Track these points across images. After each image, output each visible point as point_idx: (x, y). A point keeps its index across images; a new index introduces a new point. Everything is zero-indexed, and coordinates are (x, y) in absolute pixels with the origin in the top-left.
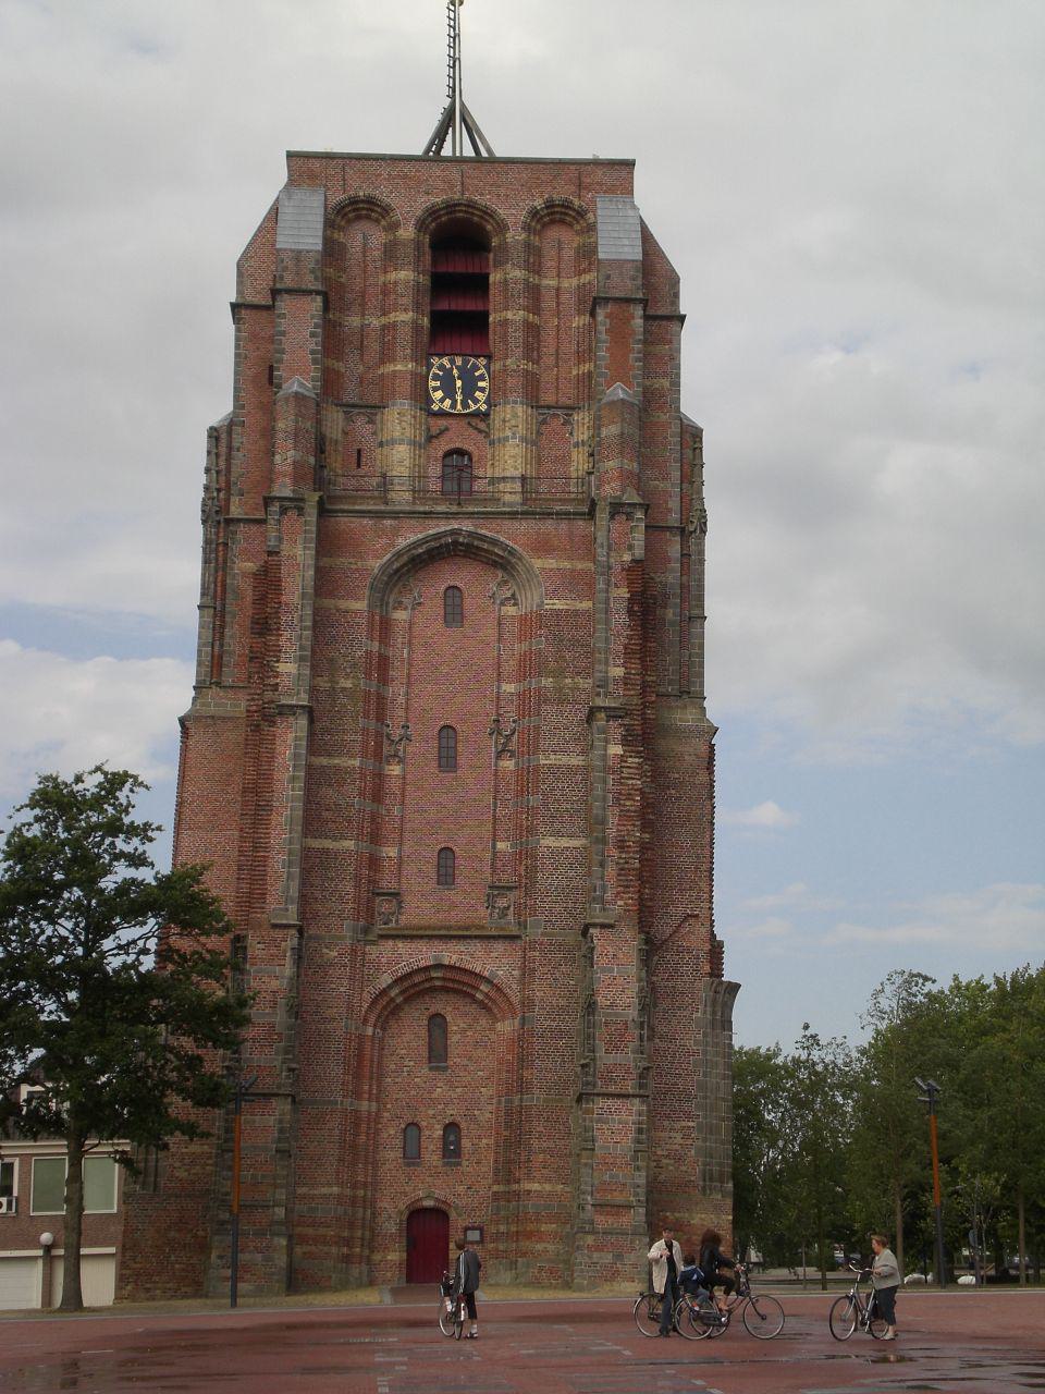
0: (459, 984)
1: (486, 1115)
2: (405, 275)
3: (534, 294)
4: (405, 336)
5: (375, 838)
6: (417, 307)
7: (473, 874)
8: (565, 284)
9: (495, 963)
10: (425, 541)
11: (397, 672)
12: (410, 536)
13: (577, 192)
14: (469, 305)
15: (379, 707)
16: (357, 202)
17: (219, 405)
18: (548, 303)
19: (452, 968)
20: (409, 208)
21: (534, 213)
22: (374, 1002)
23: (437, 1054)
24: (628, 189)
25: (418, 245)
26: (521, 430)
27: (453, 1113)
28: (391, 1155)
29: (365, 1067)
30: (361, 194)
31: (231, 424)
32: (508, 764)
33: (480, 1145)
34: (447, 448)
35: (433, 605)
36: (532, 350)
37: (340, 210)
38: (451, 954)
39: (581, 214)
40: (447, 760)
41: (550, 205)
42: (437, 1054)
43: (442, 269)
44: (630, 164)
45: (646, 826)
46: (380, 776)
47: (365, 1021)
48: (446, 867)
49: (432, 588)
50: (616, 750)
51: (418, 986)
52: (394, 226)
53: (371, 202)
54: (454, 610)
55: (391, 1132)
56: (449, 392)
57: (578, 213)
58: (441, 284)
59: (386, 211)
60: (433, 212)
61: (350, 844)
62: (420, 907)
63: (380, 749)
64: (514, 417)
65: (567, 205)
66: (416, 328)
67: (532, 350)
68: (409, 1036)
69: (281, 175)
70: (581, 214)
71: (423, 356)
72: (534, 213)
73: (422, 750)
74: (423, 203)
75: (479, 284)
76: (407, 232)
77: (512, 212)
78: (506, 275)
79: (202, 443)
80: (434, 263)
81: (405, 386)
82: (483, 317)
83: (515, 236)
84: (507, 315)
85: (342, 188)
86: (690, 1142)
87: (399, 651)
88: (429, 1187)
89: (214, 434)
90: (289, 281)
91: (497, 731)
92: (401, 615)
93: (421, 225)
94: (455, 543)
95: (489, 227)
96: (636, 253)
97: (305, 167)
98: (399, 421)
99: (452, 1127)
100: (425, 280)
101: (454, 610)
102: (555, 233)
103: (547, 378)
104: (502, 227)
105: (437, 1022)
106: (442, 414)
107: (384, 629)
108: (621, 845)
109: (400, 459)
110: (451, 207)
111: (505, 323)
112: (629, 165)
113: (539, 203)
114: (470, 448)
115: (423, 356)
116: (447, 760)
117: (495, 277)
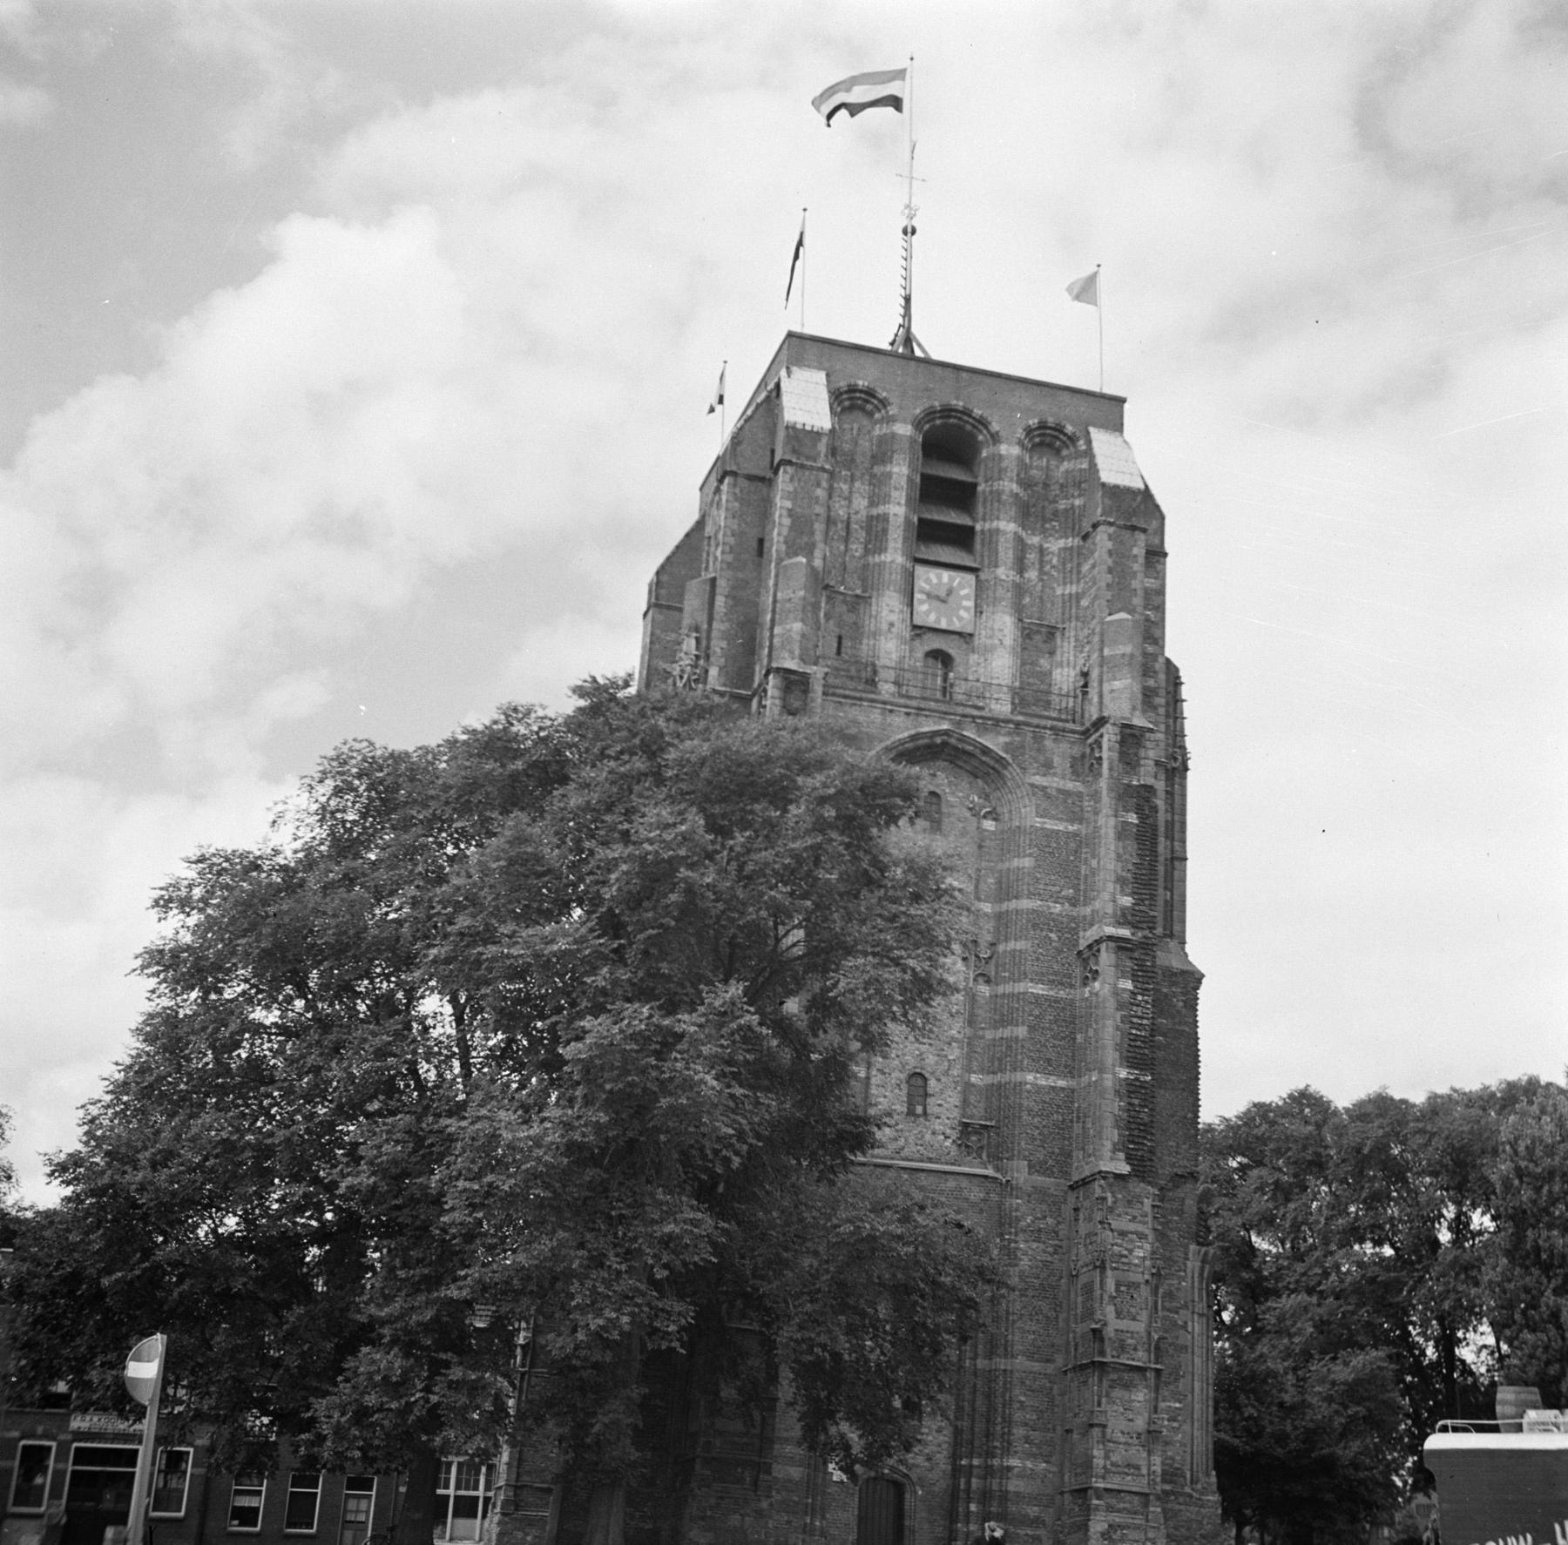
7: (946, 1105)
10: (913, 738)
13: (1066, 422)
16: (855, 391)
21: (1029, 431)
24: (1117, 426)
26: (1008, 641)
30: (860, 383)
34: (927, 648)
44: (1123, 401)
50: (1129, 985)
53: (870, 393)
57: (1070, 438)
76: (904, 429)
81: (897, 577)
86: (1175, 1424)
94: (945, 744)
95: (981, 438)
96: (1142, 486)
104: (995, 438)
110: (947, 411)
112: (1123, 401)
113: (1033, 422)
114: (951, 651)
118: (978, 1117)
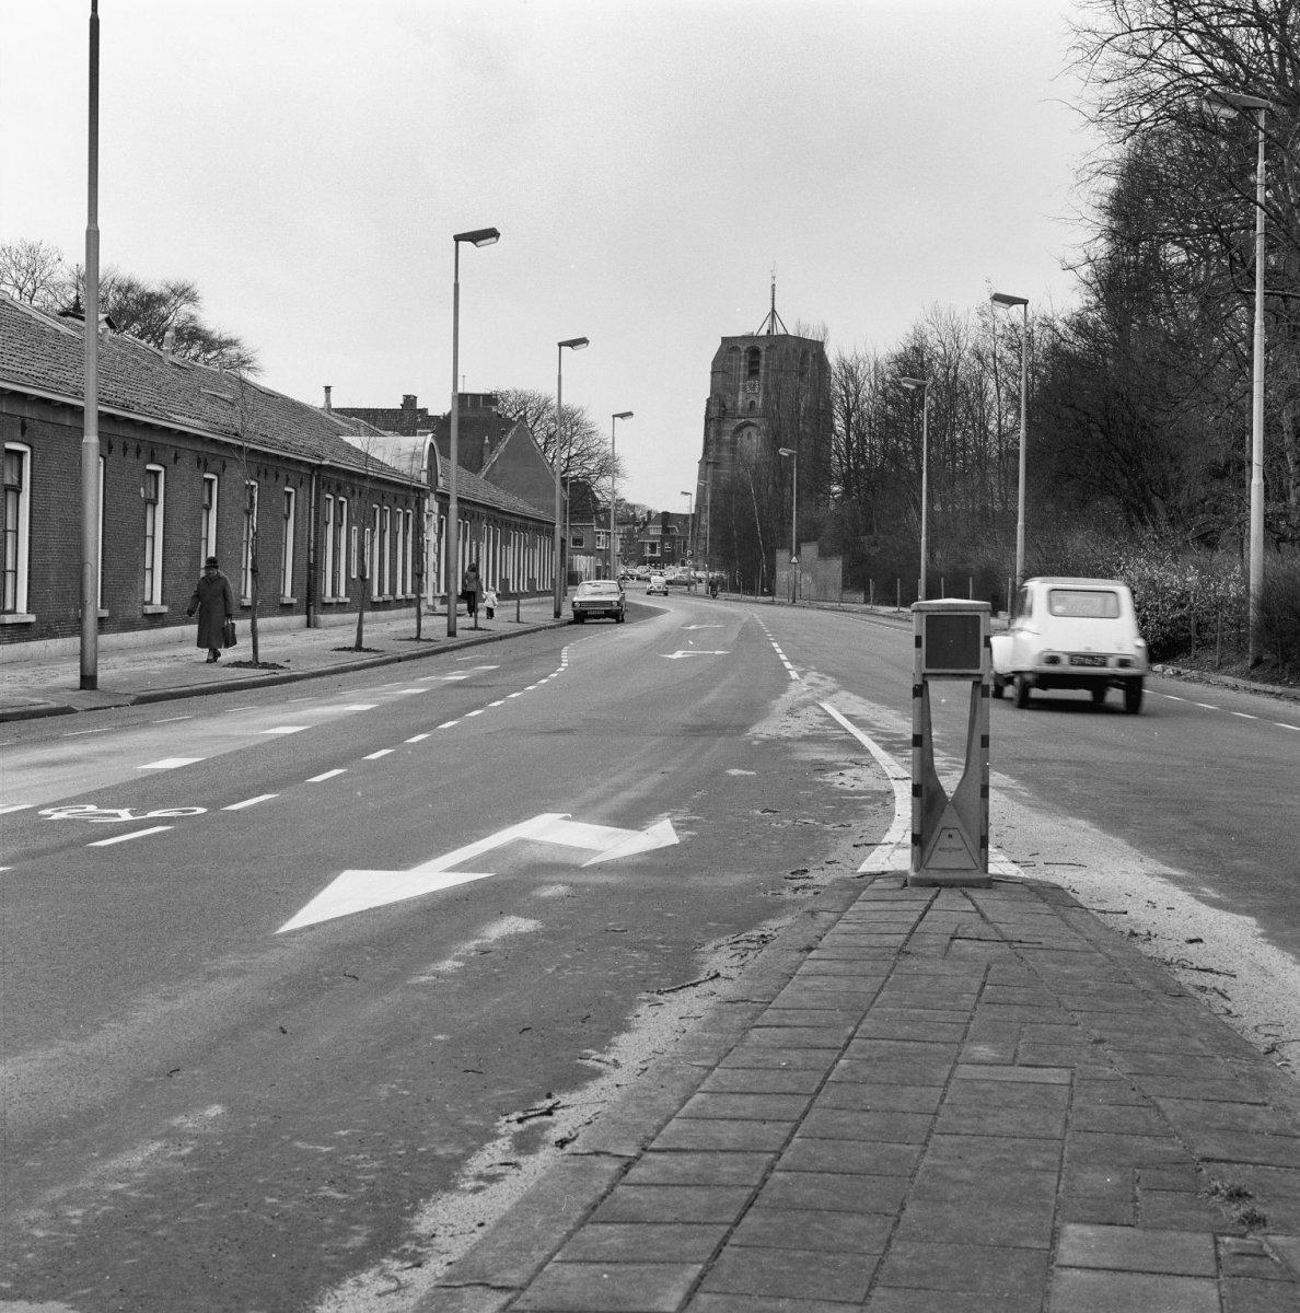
4: (742, 377)
20: (743, 348)
25: (745, 356)
49: (746, 431)
77: (762, 348)
78: (763, 362)
83: (763, 353)
84: (762, 371)
93: (746, 352)
97: (724, 340)
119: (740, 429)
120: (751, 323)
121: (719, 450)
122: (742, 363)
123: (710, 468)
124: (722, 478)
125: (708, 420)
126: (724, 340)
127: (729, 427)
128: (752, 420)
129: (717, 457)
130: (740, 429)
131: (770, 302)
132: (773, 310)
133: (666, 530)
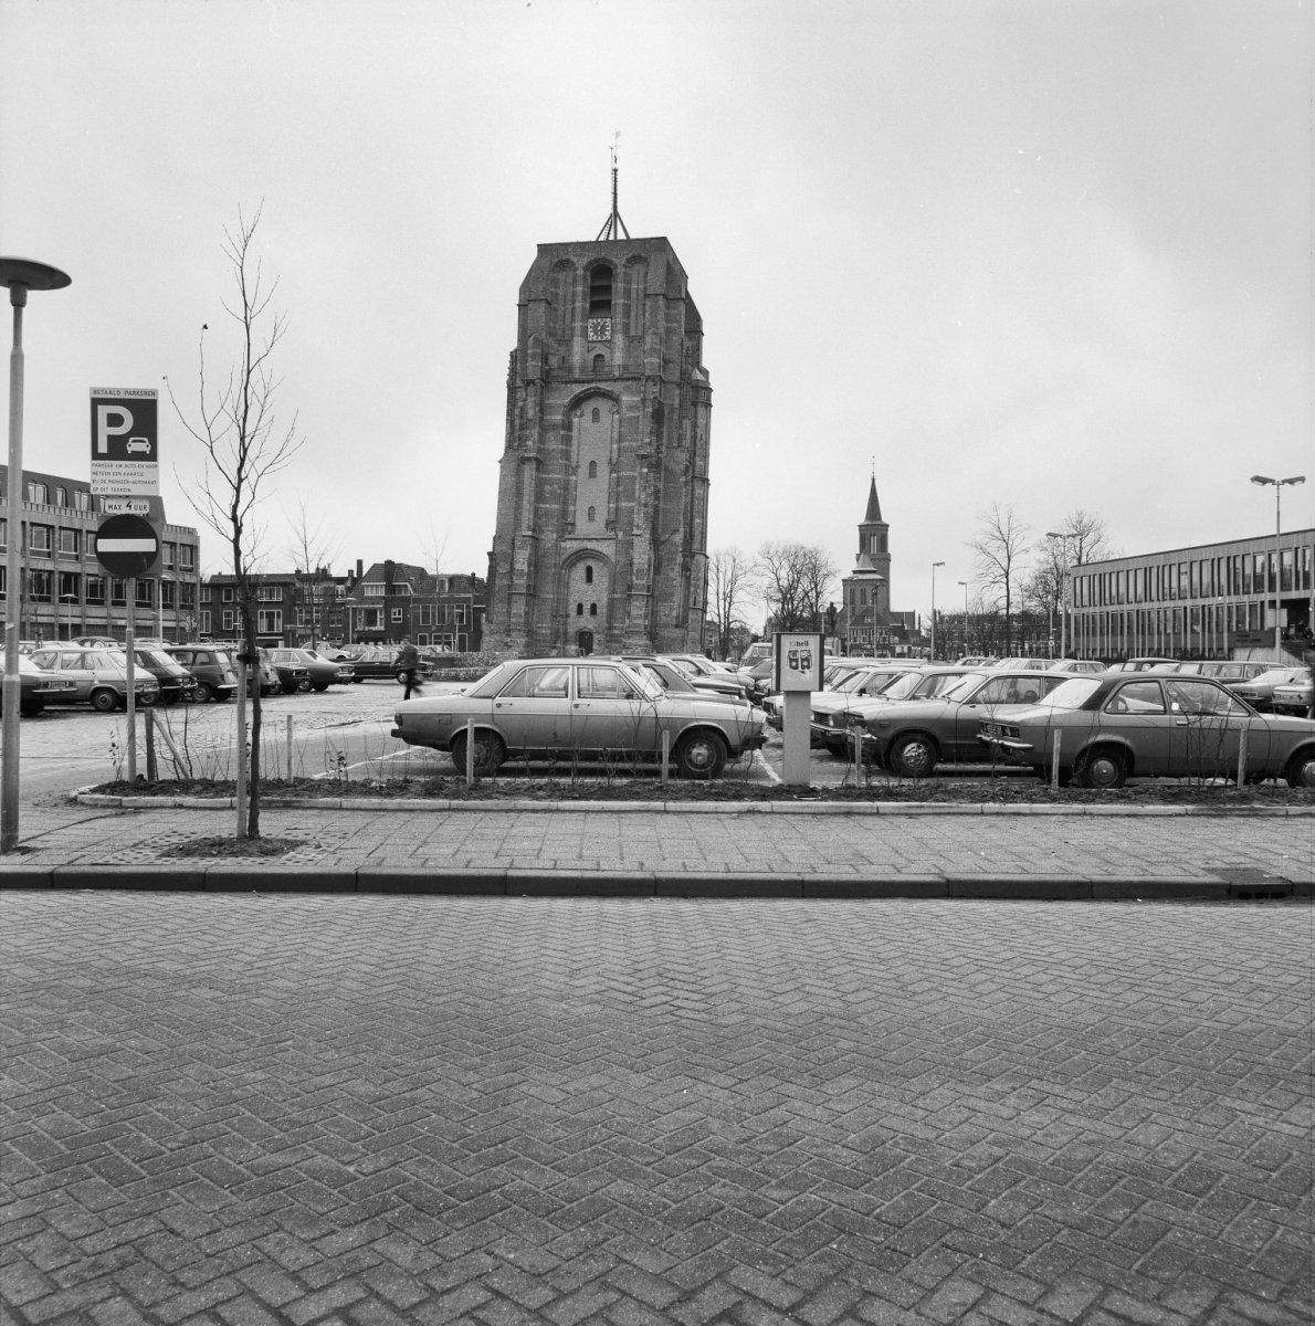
0: (597, 556)
1: (605, 600)
2: (579, 289)
3: (627, 293)
4: (578, 311)
5: (565, 503)
6: (584, 299)
7: (602, 516)
8: (640, 286)
9: (607, 549)
11: (575, 442)
12: (578, 389)
14: (605, 298)
15: (567, 455)
17: (513, 344)
18: (634, 295)
19: (591, 550)
20: (581, 262)
22: (564, 563)
23: (589, 579)
25: (584, 277)
27: (593, 600)
28: (573, 613)
29: (562, 583)
31: (516, 351)
32: (615, 475)
33: (602, 610)
35: (588, 417)
36: (627, 315)
37: (556, 265)
38: (589, 545)
39: (646, 260)
40: (592, 474)
41: (634, 257)
42: (589, 579)
43: (596, 284)
45: (657, 498)
46: (567, 482)
47: (562, 568)
48: (591, 517)
49: (588, 407)
50: (646, 470)
51: (581, 555)
52: (577, 269)
53: (567, 261)
54: (596, 415)
55: (573, 608)
56: (596, 332)
58: (594, 290)
59: (573, 264)
60: (590, 263)
61: (556, 506)
62: (583, 526)
63: (571, 469)
64: (619, 340)
65: (640, 257)
66: (583, 309)
67: (627, 315)
68: (579, 572)
69: (534, 254)
70: (646, 260)
71: (585, 319)
72: (628, 260)
73: (584, 470)
74: (585, 261)
75: (608, 289)
76: (580, 272)
77: (619, 261)
78: (619, 286)
79: (509, 358)
80: (592, 281)
81: (578, 332)
82: (610, 301)
83: (620, 270)
84: (618, 301)
85: (554, 258)
87: (575, 434)
88: (587, 622)
89: (513, 355)
90: (533, 297)
91: (610, 463)
92: (576, 420)
93: (585, 269)
97: (543, 249)
98: (578, 346)
99: (594, 607)
100: (588, 290)
101: (596, 415)
102: (637, 267)
103: (632, 325)
104: (616, 267)
105: (589, 571)
106: (593, 342)
107: (568, 426)
108: (646, 506)
109: (576, 359)
110: (596, 260)
111: (615, 304)
115: (585, 319)
116: (592, 474)
117: (614, 286)
118: (612, 518)
119: (577, 402)
120: (582, 225)
121: (542, 439)
122: (579, 289)
123: (529, 471)
124: (547, 488)
125: (518, 383)
126: (543, 249)
127: (562, 397)
128: (604, 386)
129: (540, 450)
130: (577, 402)
131: (611, 196)
132: (616, 214)
133: (391, 589)
